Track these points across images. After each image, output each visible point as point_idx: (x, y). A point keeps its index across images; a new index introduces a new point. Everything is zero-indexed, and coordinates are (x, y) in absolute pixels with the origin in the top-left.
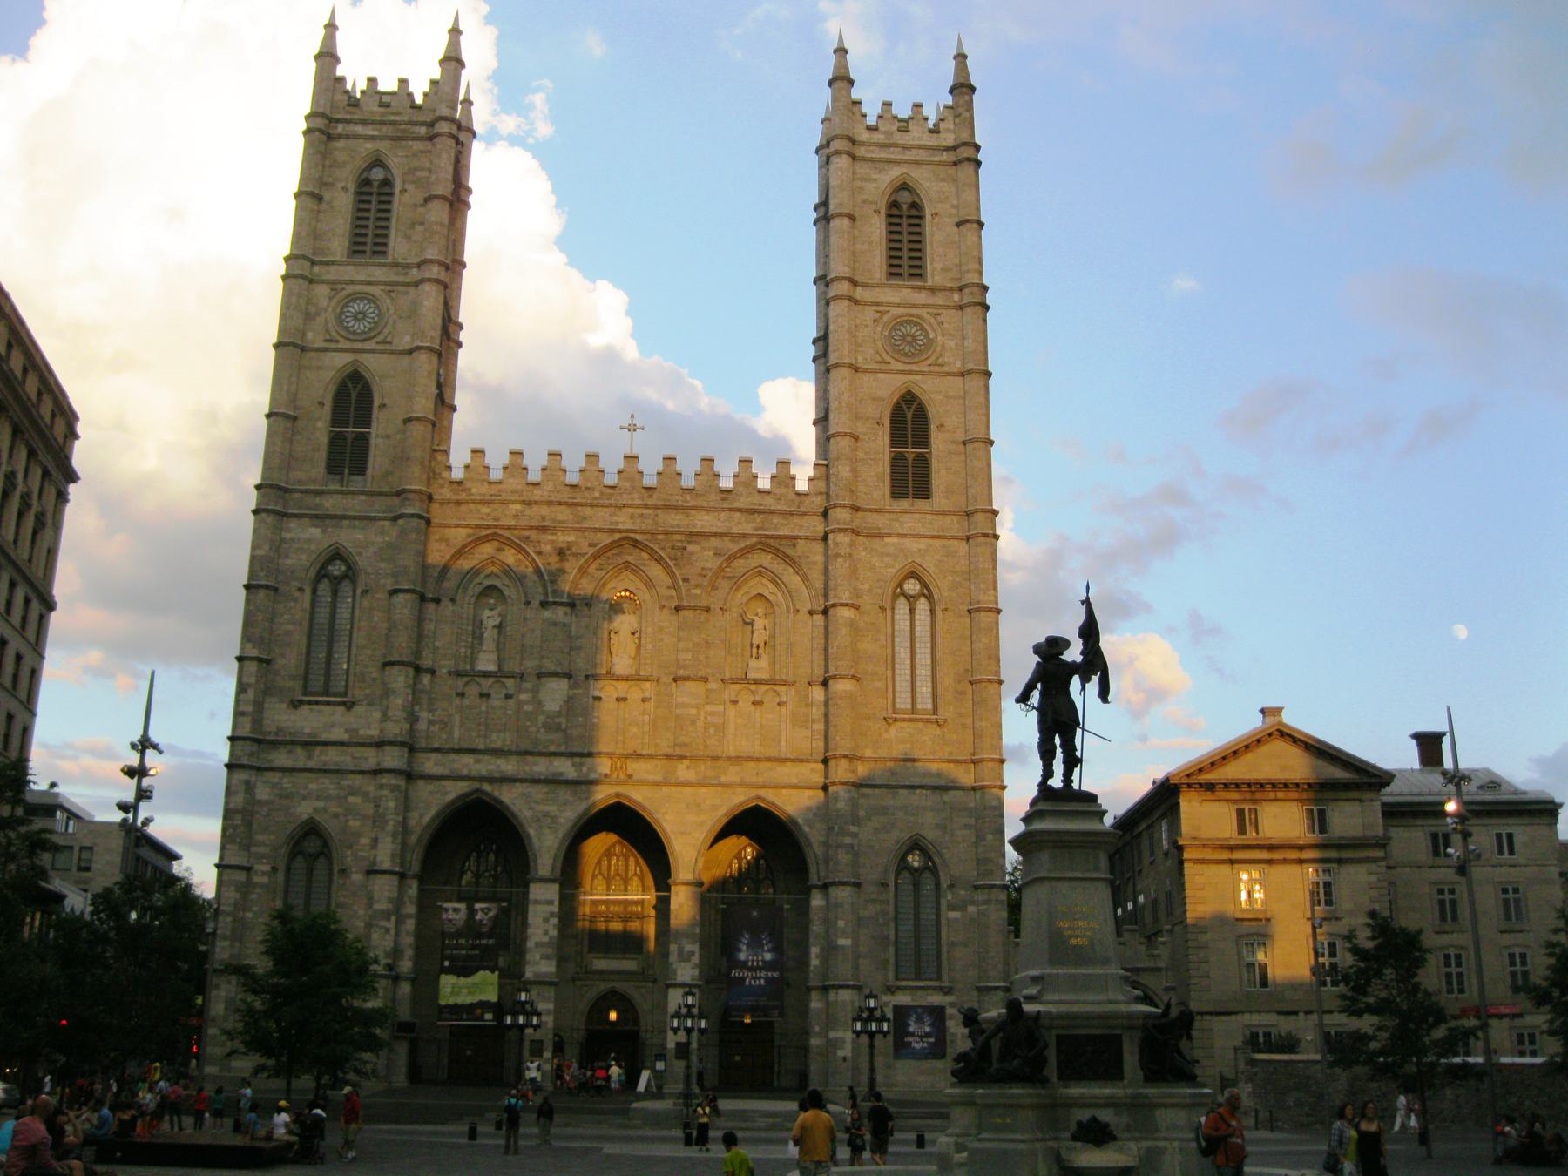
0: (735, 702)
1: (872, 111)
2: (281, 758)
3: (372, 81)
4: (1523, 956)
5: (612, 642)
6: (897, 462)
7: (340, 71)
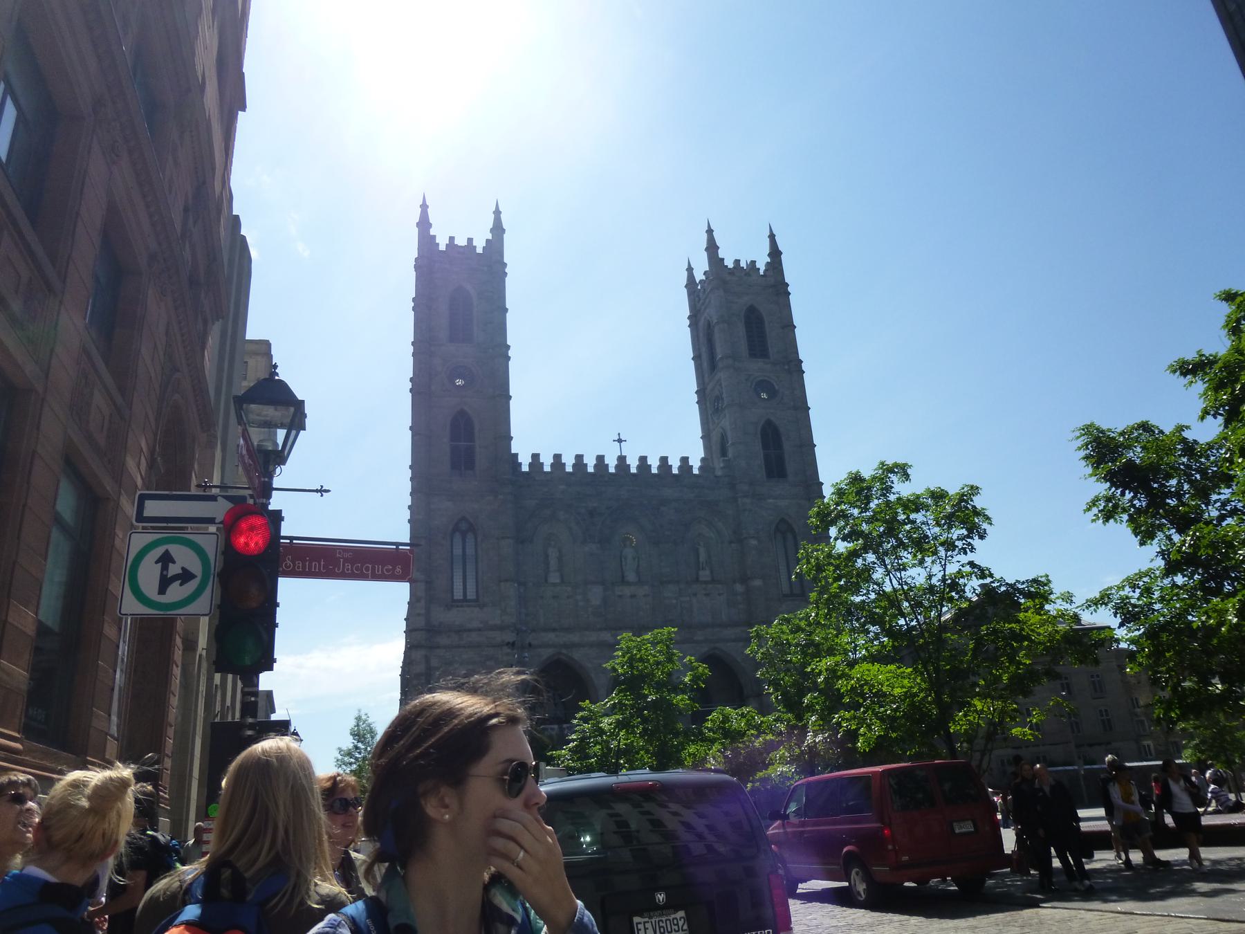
0: (695, 595)
1: (729, 263)
2: (443, 640)
3: (452, 239)
4: (1106, 711)
5: (624, 563)
6: (767, 459)
7: (432, 232)
